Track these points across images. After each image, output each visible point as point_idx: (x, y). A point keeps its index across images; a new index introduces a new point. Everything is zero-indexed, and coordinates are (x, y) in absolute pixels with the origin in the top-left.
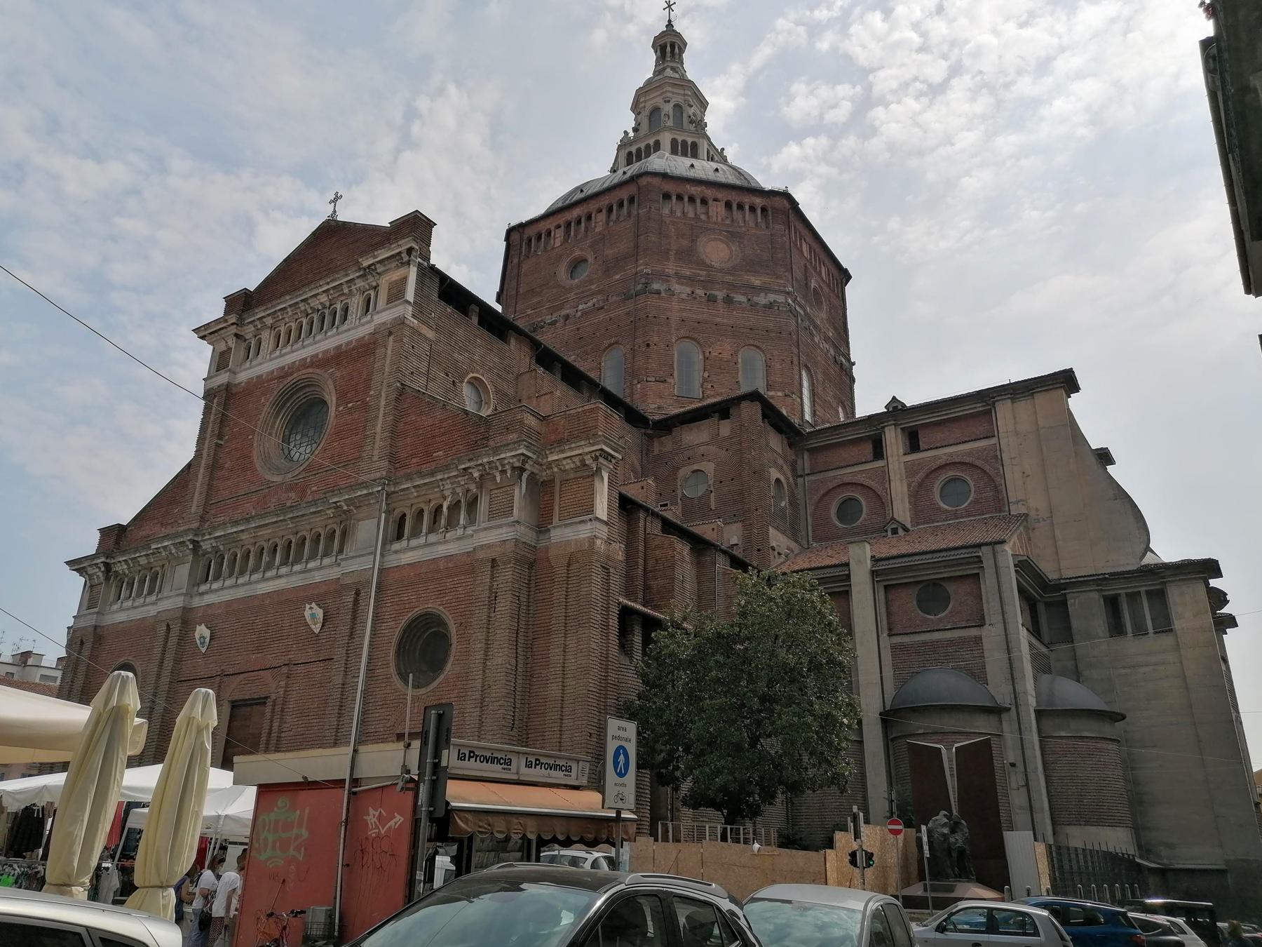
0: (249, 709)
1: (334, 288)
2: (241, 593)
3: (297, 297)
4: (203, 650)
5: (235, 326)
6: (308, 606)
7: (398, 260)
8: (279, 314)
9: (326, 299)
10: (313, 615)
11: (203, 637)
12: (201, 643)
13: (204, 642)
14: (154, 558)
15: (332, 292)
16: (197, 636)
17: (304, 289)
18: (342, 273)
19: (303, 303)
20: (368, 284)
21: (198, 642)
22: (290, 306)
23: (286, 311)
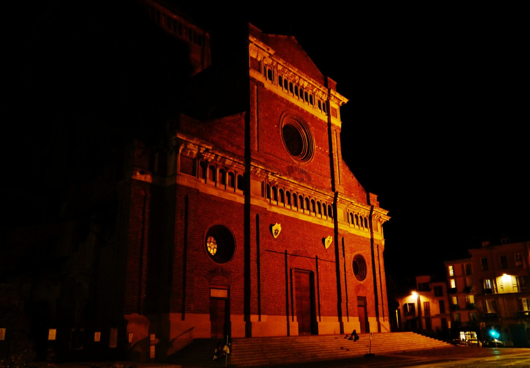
0: (299, 274)
1: (312, 85)
2: (291, 214)
3: (299, 73)
4: (275, 237)
5: (268, 55)
6: (329, 237)
7: (338, 102)
8: (287, 70)
9: (306, 85)
10: (329, 241)
11: (278, 231)
12: (275, 233)
13: (277, 233)
14: (237, 165)
15: (310, 85)
16: (274, 228)
17: (305, 74)
18: (320, 85)
19: (298, 77)
20: (322, 96)
21: (274, 232)
22: (294, 73)
23: (290, 72)
